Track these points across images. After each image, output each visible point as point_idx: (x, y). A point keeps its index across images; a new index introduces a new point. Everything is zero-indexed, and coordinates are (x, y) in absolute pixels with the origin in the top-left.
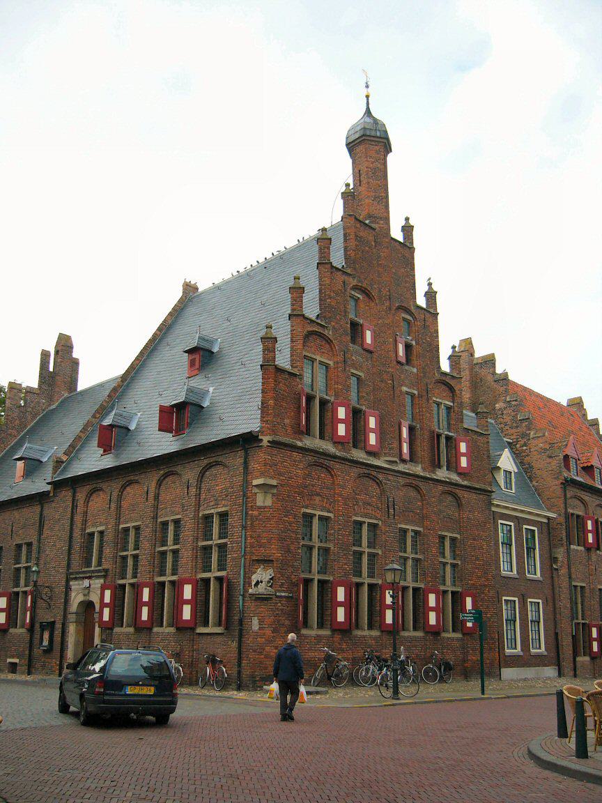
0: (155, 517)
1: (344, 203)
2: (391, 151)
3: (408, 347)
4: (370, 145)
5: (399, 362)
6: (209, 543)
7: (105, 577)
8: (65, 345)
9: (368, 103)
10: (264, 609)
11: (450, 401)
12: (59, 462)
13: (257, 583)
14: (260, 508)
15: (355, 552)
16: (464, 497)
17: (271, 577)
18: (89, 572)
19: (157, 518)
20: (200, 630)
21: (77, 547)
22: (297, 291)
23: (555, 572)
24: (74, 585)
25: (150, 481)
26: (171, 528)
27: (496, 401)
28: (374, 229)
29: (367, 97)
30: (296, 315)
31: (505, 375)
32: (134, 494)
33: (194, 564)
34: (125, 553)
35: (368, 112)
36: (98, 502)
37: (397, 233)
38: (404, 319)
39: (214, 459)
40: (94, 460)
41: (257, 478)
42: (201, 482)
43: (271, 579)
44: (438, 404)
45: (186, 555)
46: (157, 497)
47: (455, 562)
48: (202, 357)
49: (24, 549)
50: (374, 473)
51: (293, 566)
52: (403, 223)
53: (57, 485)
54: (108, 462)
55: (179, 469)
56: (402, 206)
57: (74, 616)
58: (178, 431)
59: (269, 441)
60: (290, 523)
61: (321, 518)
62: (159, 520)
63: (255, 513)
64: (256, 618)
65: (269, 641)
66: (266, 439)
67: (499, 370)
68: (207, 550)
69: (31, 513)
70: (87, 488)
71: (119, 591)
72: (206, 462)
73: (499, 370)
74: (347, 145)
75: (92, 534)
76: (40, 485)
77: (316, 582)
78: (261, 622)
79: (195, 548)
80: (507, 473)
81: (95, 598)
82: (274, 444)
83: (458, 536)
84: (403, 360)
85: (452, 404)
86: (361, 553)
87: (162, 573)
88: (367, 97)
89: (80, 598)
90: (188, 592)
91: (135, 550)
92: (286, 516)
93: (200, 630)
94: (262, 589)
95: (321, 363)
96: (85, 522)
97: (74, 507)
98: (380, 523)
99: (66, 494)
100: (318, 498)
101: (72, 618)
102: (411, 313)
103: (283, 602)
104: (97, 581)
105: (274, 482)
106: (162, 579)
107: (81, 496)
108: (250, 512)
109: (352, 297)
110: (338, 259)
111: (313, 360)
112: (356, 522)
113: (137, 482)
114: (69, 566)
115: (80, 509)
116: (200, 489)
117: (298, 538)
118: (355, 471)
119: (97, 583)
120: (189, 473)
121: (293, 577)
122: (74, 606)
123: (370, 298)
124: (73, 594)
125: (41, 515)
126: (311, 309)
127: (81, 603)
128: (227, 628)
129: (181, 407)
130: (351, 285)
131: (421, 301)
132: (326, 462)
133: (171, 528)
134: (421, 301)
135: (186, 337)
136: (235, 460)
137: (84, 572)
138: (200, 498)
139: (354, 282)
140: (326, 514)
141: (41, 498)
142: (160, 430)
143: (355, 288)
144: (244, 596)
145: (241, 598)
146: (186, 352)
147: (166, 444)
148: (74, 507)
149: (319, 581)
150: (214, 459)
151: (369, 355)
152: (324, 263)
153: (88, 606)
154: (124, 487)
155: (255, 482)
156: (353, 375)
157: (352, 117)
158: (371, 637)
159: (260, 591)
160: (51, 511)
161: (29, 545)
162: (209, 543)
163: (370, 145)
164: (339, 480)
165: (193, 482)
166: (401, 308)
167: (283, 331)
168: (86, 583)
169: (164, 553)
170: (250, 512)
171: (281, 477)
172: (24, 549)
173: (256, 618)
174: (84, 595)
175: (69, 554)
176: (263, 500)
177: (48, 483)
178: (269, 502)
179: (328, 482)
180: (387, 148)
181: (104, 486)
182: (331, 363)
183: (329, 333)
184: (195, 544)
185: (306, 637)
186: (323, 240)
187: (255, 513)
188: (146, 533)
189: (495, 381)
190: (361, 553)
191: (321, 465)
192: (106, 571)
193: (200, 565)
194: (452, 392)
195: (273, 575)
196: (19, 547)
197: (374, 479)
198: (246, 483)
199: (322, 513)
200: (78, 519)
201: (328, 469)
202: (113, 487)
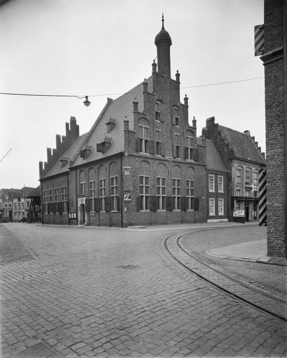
0: (98, 179)
3: (177, 119)
4: (163, 41)
5: (173, 125)
6: (113, 186)
7: (86, 197)
8: (73, 121)
9: (163, 23)
12: (71, 162)
14: (126, 175)
15: (157, 187)
18: (82, 195)
20: (112, 211)
21: (78, 188)
22: (136, 104)
23: (229, 190)
24: (79, 200)
25: (96, 167)
26: (103, 182)
28: (164, 77)
29: (163, 20)
30: (136, 112)
31: (218, 124)
32: (92, 172)
34: (91, 190)
35: (163, 28)
36: (83, 174)
37: (173, 77)
38: (176, 109)
39: (112, 161)
40: (80, 161)
44: (188, 138)
45: (107, 190)
47: (192, 188)
48: (112, 125)
49: (64, 189)
50: (164, 162)
52: (176, 73)
53: (71, 169)
54: (85, 162)
55: (104, 164)
57: (79, 208)
58: (103, 153)
60: (135, 180)
61: (145, 177)
62: (100, 180)
66: (126, 154)
67: (216, 122)
68: (113, 188)
69: (64, 178)
70: (80, 170)
73: (216, 122)
74: (155, 43)
75: (82, 184)
76: (66, 169)
77: (145, 197)
79: (109, 187)
81: (84, 203)
82: (129, 155)
83: (194, 180)
84: (174, 123)
86: (159, 187)
87: (102, 195)
88: (163, 20)
89: (80, 203)
91: (94, 188)
93: (112, 211)
95: (145, 128)
96: (80, 181)
97: (76, 176)
98: (166, 178)
99: (74, 172)
100: (145, 172)
101: (79, 209)
102: (179, 107)
104: (84, 198)
105: (129, 167)
106: (101, 197)
107: (78, 172)
109: (156, 103)
110: (150, 90)
111: (142, 127)
112: (157, 178)
113: (93, 168)
114: (77, 194)
117: (138, 184)
118: (157, 162)
119: (84, 199)
120: (106, 165)
122: (79, 206)
124: (79, 202)
126: (141, 109)
127: (81, 204)
128: (118, 210)
129: (103, 143)
133: (103, 182)
134: (182, 102)
135: (106, 120)
137: (81, 196)
140: (147, 176)
141: (66, 173)
142: (97, 151)
143: (158, 100)
146: (106, 124)
147: (100, 156)
148: (76, 176)
149: (146, 196)
150: (112, 161)
152: (145, 92)
153: (83, 205)
154: (89, 170)
155: (124, 168)
156: (157, 131)
158: (163, 212)
160: (70, 176)
161: (65, 187)
162: (113, 186)
163: (163, 41)
164: (152, 166)
165: (108, 168)
167: (131, 119)
168: (81, 198)
169: (101, 189)
172: (64, 189)
174: (82, 202)
175: (76, 190)
177: (69, 169)
178: (128, 174)
179: (148, 166)
180: (170, 43)
181: (84, 169)
182: (148, 127)
183: (148, 117)
185: (142, 212)
186: (145, 84)
188: (96, 183)
190: (159, 187)
191: (145, 161)
196: (63, 188)
197: (164, 164)
198: (121, 168)
200: (78, 179)
201: (148, 162)
202: (86, 169)
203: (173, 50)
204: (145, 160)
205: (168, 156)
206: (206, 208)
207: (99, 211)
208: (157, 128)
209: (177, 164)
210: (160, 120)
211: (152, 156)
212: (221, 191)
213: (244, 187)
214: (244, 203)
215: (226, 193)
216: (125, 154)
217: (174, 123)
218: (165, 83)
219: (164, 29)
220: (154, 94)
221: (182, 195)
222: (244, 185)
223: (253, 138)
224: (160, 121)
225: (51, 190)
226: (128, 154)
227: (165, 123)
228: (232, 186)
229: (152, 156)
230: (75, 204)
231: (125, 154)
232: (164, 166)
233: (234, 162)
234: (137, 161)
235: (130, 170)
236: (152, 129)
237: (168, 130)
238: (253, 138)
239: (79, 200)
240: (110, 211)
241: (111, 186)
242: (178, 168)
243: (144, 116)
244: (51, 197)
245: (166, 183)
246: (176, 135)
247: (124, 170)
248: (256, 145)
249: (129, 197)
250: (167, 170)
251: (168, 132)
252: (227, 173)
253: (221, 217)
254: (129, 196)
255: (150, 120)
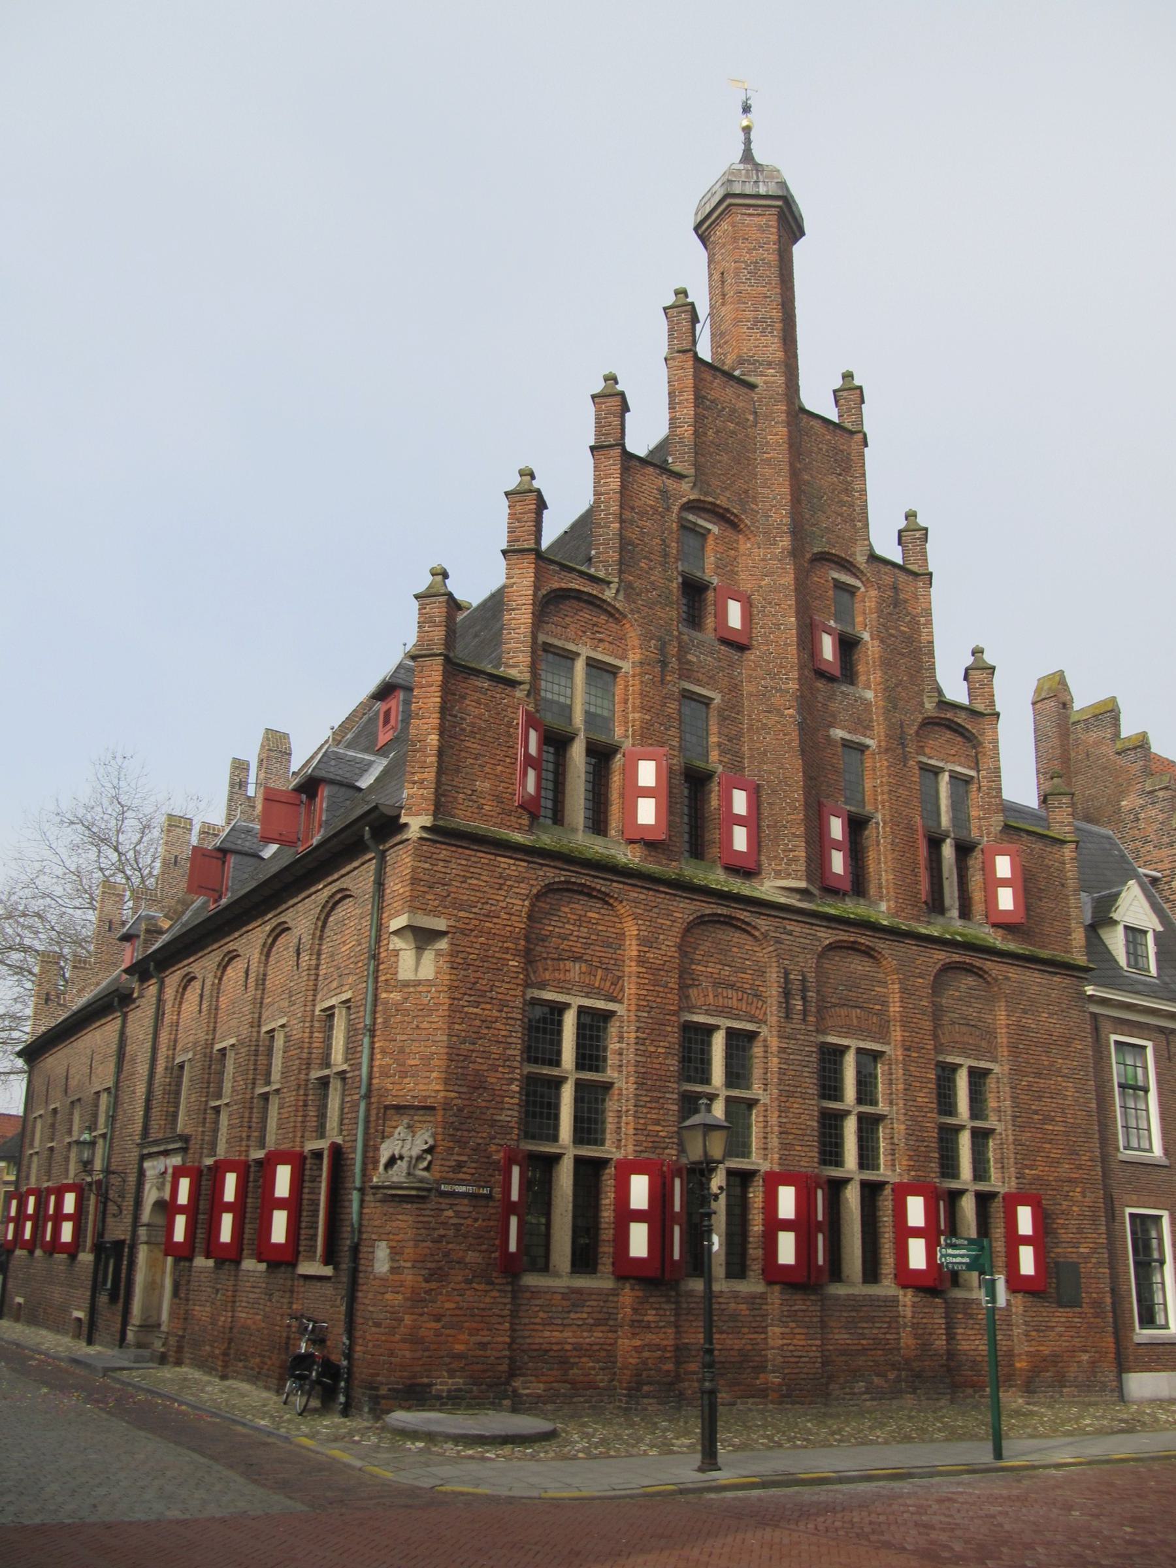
1: (671, 330)
7: (184, 1150)
10: (404, 1221)
11: (970, 768)
13: (392, 1161)
14: (406, 984)
16: (1007, 978)
17: (426, 1147)
19: (259, 1026)
27: (1122, 793)
33: (300, 1119)
41: (397, 914)
42: (321, 938)
43: (425, 1151)
46: (262, 981)
51: (493, 1123)
59: (424, 828)
63: (396, 996)
64: (383, 1244)
65: (417, 1300)
66: (416, 823)
71: (207, 1183)
72: (326, 893)
78: (395, 1253)
80: (1134, 934)
90: (283, 1177)
92: (477, 1004)
94: (398, 1174)
103: (461, 1208)
108: (384, 995)
115: (168, 1019)
116: (319, 954)
120: (301, 916)
121: (494, 1148)
125: (122, 1033)
132: (599, 884)
136: (359, 877)
138: (317, 975)
139: (686, 491)
144: (362, 1190)
145: (355, 1195)
151: (735, 655)
154: (223, 967)
159: (395, 1179)
166: (824, 558)
170: (384, 995)
171: (461, 914)
173: (383, 1244)
176: (415, 966)
184: (303, 1077)
187: (396, 996)
189: (1119, 753)
192: (186, 1139)
193: (312, 1122)
195: (431, 1142)
198: (380, 927)
199: (587, 1002)
200: (164, 1036)
207: (231, 1261)
216: (403, 820)
225: (55, 1111)
226: (427, 821)
230: (128, 1204)
231: (403, 820)
234: (501, 883)
235: (443, 944)
239: (153, 1168)
240: (294, 1265)
241: (316, 1074)
243: (588, 588)
244: (51, 1149)
247: (397, 943)
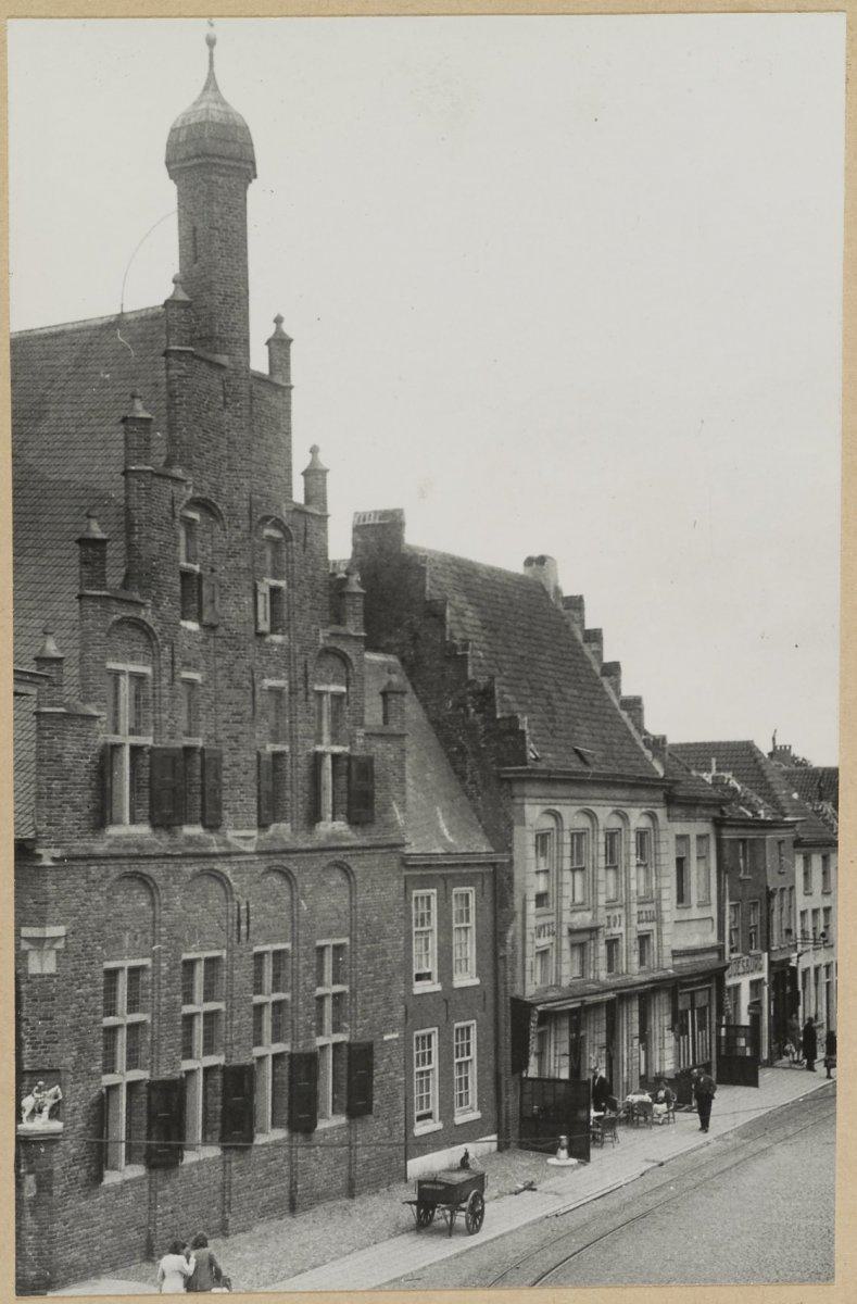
2: (255, 176)
23: (501, 963)
28: (221, 367)
35: (211, 84)
56: (273, 293)
74: (168, 164)
85: (344, 689)
88: (211, 43)
123: (213, 515)
130: (184, 502)
131: (259, 362)
157: (177, 102)
194: (345, 665)
203: (261, 203)
204: (135, 870)
205: (236, 828)
206: (402, 1094)
208: (187, 665)
209: (276, 862)
210: (199, 618)
211: (162, 843)
212: (466, 978)
213: (565, 932)
214: (566, 1024)
215: (489, 984)
217: (264, 626)
218: (225, 403)
219: (216, 89)
220: (178, 472)
221: (295, 1039)
222: (566, 917)
223: (576, 604)
224: (203, 626)
227: (221, 631)
228: (514, 937)
229: (162, 843)
232: (218, 886)
233: (526, 800)
236: (165, 681)
237: (237, 675)
238: (576, 604)
242: (276, 881)
245: (222, 986)
246: (271, 690)
248: (594, 647)
249: (52, 1110)
250: (232, 911)
251: (239, 686)
252: (494, 864)
253: (471, 1132)
254: (50, 1102)
255: (156, 629)
